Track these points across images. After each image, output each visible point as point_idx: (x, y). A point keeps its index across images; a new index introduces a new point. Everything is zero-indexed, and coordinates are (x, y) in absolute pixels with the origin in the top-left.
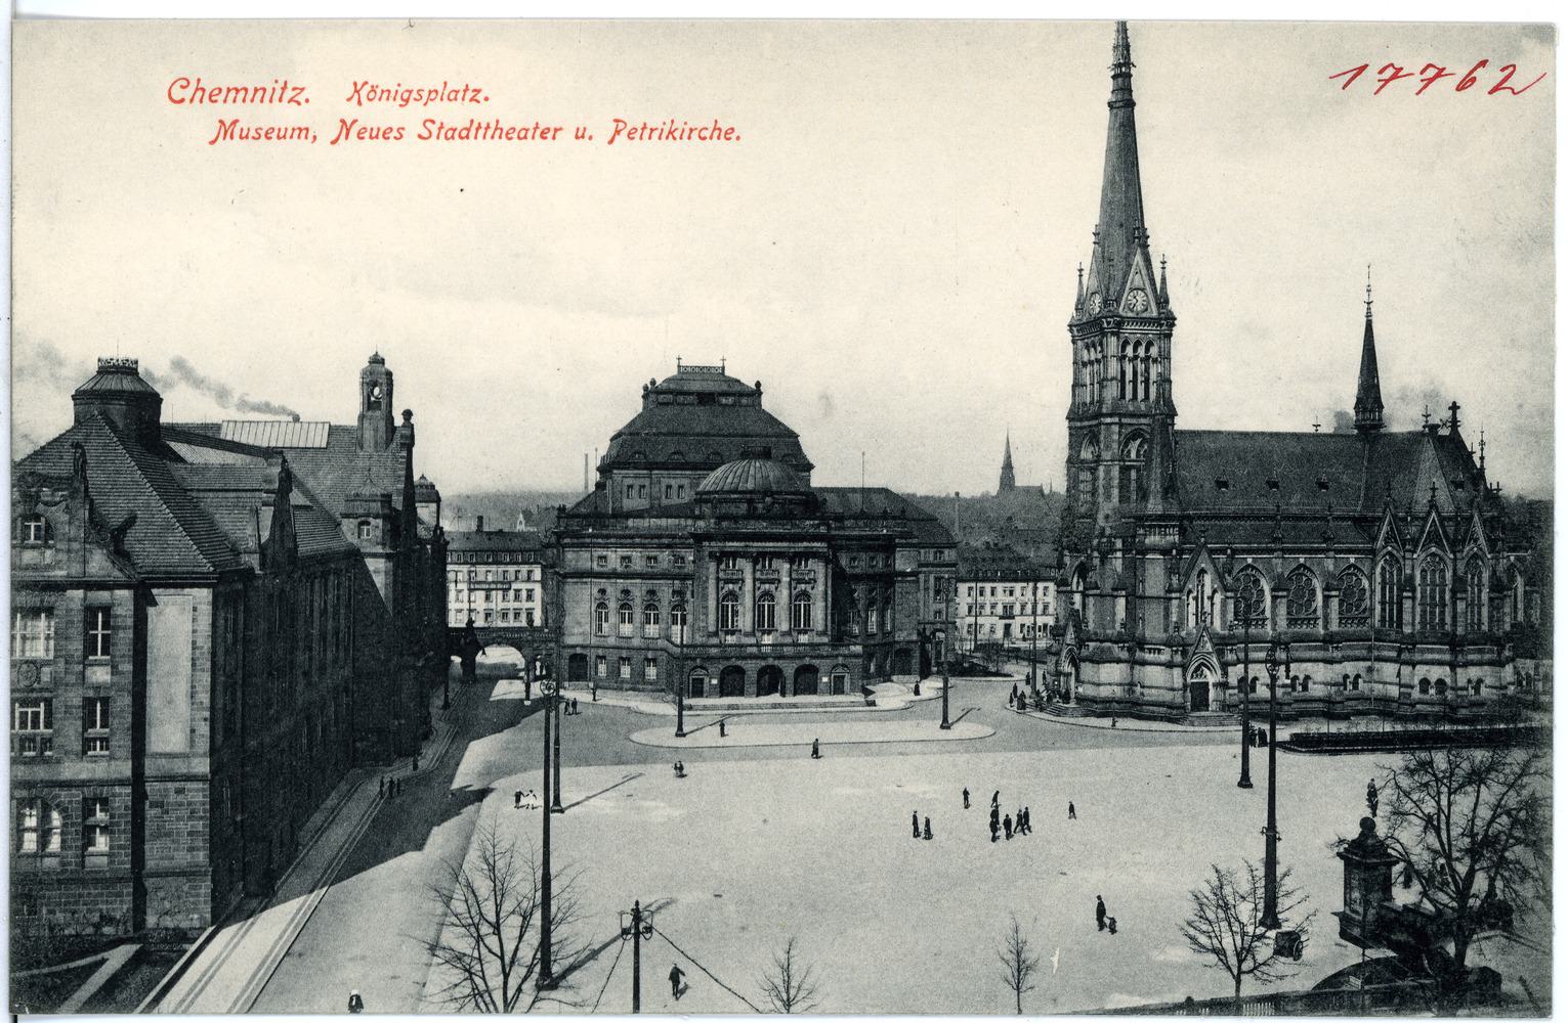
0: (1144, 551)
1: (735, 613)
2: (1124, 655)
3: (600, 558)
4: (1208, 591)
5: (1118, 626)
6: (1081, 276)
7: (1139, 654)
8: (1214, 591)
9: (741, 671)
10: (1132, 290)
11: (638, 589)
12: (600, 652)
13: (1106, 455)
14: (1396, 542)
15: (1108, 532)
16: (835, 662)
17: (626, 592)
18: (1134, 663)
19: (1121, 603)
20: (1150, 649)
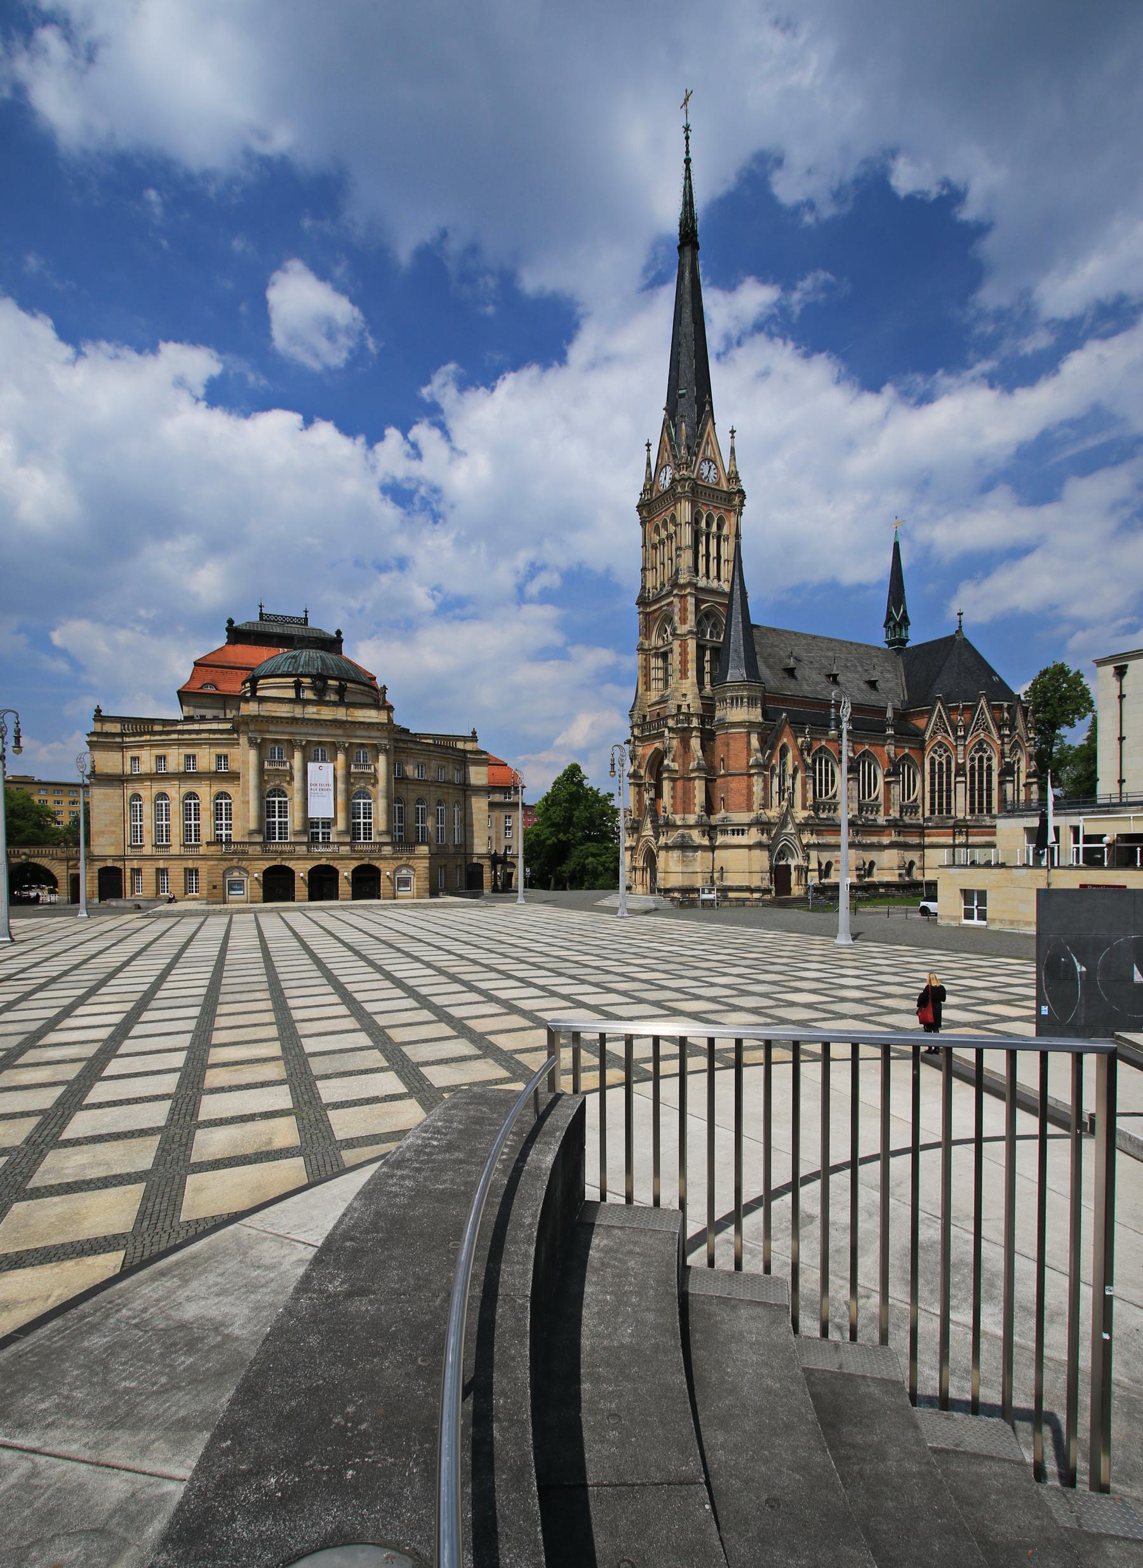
0: (725, 725)
1: (283, 807)
2: (706, 842)
3: (135, 759)
4: (790, 771)
5: (697, 809)
6: (649, 450)
7: (720, 839)
8: (795, 770)
9: (290, 873)
10: (704, 460)
11: (175, 792)
12: (136, 864)
13: (682, 629)
14: (946, 731)
15: (684, 710)
16: (400, 863)
17: (163, 796)
18: (712, 848)
19: (699, 787)
20: (733, 831)
